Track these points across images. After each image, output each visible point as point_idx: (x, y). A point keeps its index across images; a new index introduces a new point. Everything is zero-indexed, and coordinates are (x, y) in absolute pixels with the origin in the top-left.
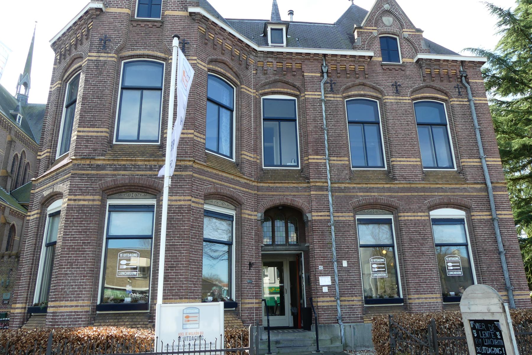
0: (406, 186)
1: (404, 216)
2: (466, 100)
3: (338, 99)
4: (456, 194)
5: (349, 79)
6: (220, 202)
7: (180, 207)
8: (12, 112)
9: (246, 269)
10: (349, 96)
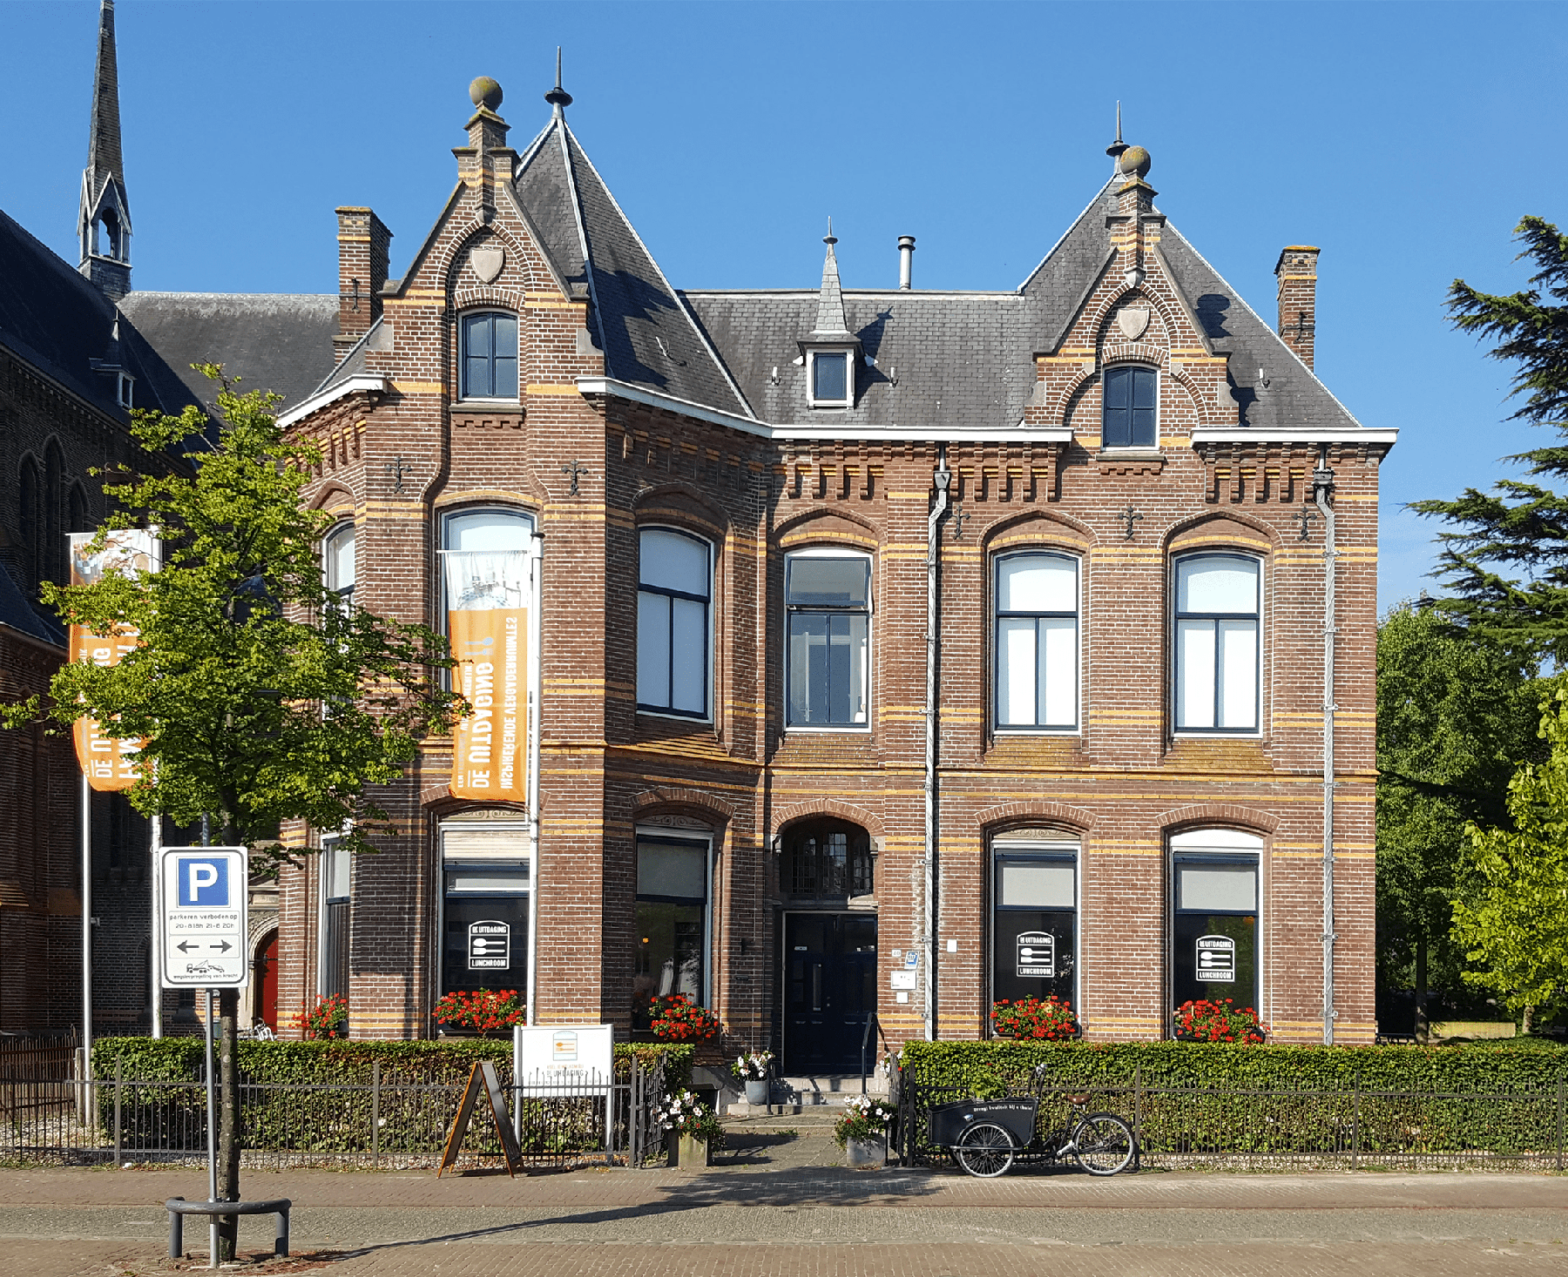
4: (1240, 797)
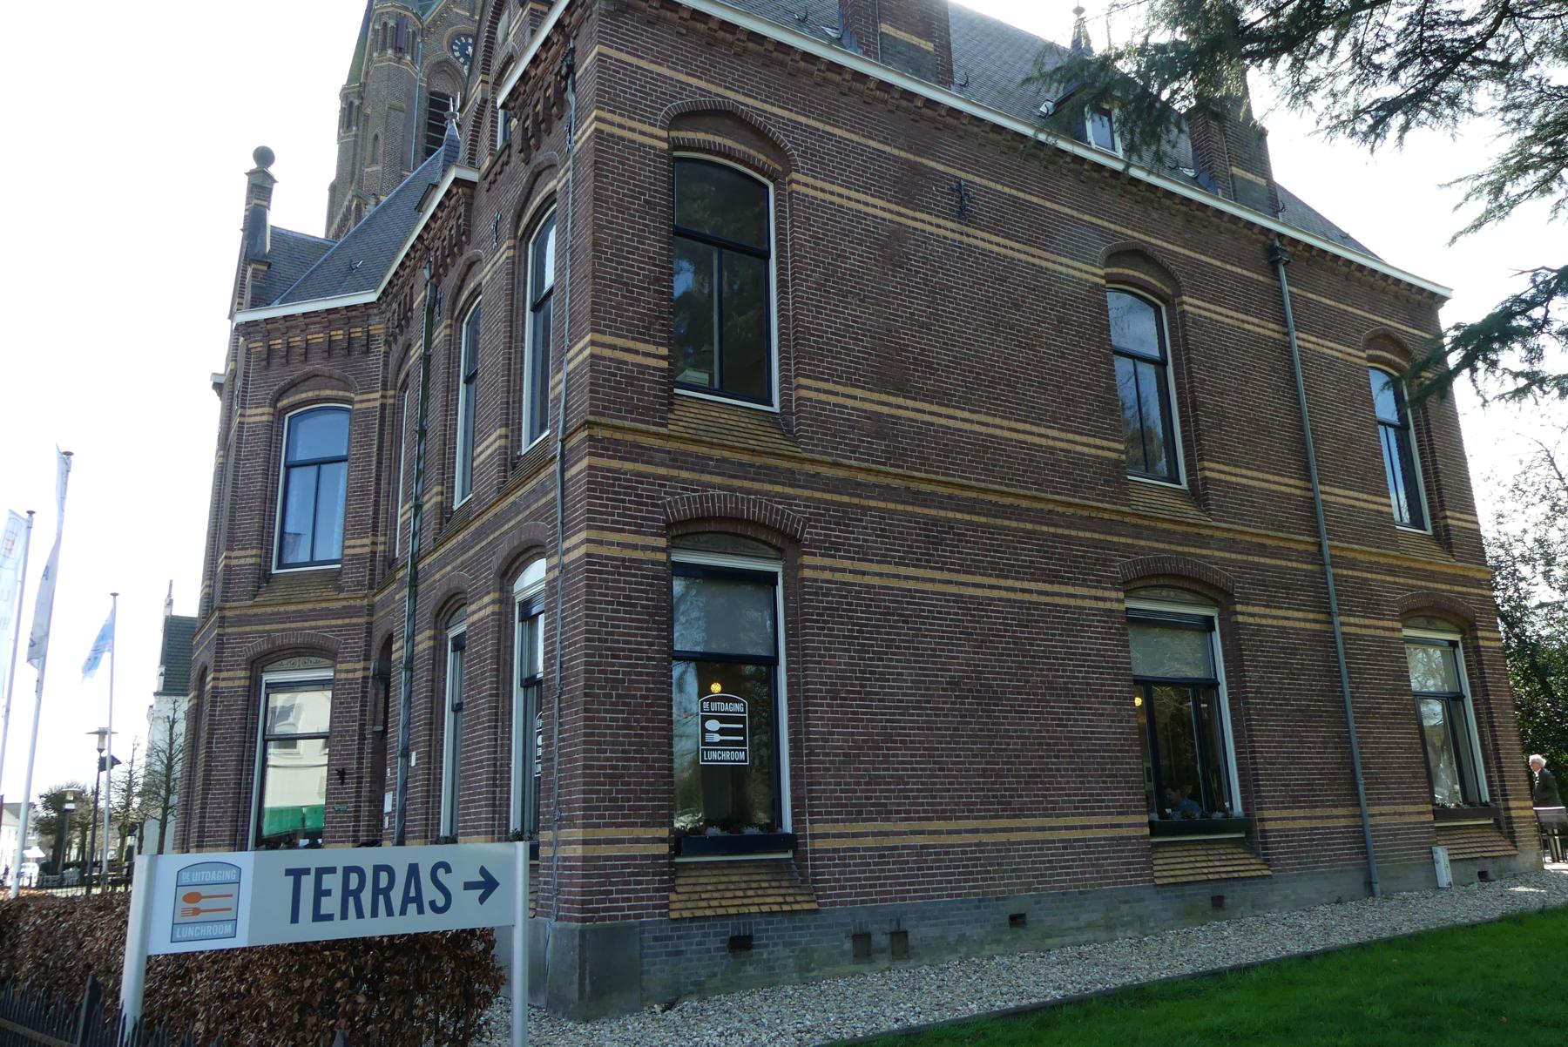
6: (298, 661)
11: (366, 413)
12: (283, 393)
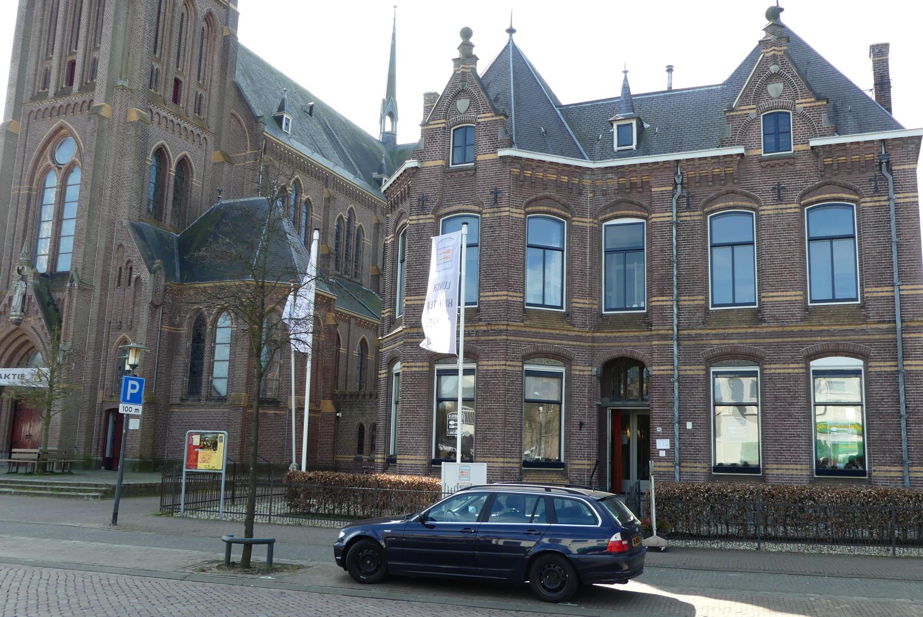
0: (776, 329)
1: (770, 369)
2: (885, 198)
3: (696, 218)
4: (847, 338)
5: (713, 188)
6: (544, 360)
7: (496, 371)
8: (375, 175)
9: (575, 429)
10: (713, 211)
11: (583, 229)
12: (529, 203)
